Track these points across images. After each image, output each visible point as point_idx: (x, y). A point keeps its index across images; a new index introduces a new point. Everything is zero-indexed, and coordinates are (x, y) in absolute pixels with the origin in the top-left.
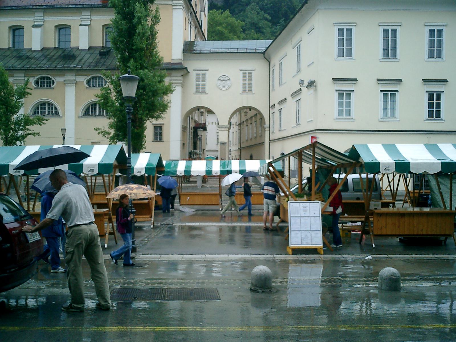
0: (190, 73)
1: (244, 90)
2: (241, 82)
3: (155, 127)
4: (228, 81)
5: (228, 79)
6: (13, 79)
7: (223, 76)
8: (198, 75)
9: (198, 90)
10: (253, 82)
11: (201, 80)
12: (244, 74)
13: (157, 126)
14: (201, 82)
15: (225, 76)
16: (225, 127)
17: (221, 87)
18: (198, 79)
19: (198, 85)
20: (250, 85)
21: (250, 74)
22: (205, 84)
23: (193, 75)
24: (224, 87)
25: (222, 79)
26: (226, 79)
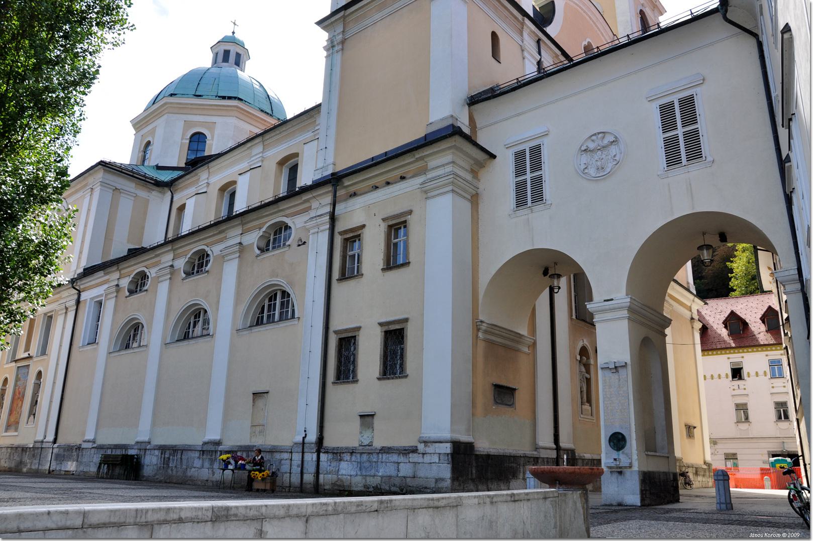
0: (496, 159)
1: (672, 159)
2: (659, 137)
3: (386, 332)
4: (613, 147)
5: (612, 139)
7: (594, 138)
8: (519, 157)
9: (521, 202)
10: (703, 125)
12: (666, 111)
13: (392, 327)
15: (601, 135)
16: (621, 308)
17: (592, 172)
18: (520, 170)
19: (520, 188)
20: (693, 139)
21: (688, 104)
22: (540, 177)
25: (592, 146)
26: (606, 142)
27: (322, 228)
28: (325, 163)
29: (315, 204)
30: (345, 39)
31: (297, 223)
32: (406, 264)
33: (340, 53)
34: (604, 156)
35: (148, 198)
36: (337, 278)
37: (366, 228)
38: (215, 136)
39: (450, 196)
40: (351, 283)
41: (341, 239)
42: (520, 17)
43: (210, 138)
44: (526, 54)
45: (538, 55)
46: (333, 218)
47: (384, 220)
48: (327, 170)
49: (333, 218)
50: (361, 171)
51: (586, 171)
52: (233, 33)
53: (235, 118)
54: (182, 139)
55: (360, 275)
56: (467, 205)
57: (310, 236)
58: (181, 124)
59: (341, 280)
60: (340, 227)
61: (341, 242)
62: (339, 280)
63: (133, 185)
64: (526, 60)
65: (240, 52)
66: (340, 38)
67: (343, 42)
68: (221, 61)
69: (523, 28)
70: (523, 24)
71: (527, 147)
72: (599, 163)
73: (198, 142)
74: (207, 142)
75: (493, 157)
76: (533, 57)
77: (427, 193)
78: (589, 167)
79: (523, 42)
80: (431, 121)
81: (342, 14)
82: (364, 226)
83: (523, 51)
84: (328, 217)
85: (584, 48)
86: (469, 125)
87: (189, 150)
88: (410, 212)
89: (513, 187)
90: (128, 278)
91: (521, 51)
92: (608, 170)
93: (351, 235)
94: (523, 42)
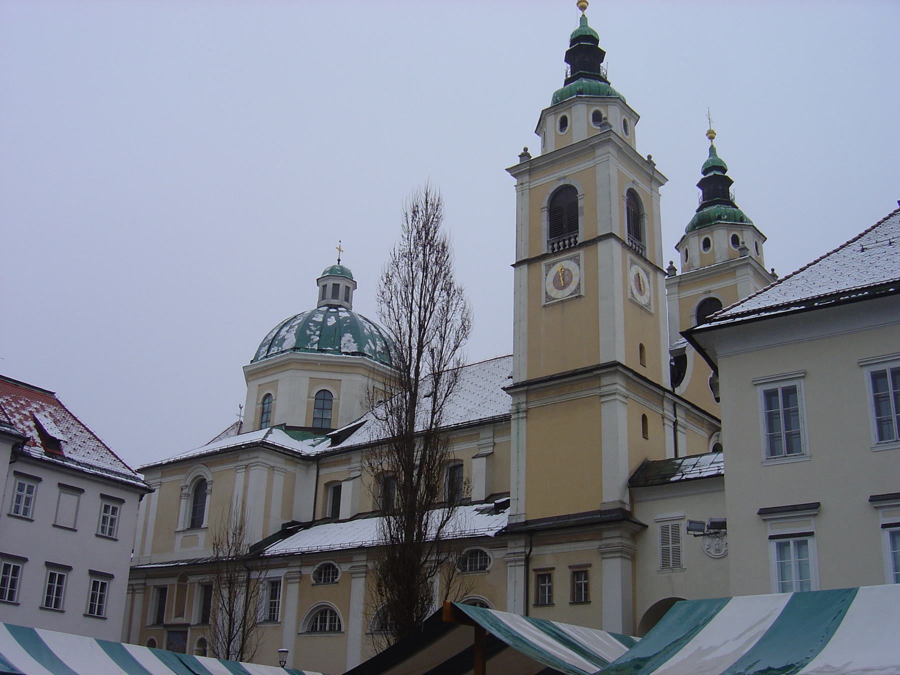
0: (649, 527)
6: (350, 566)
8: (665, 530)
9: (665, 564)
11: (670, 541)
14: (671, 546)
17: (712, 551)
18: (665, 541)
19: (665, 552)
23: (654, 534)
24: (718, 550)
27: (518, 563)
28: (517, 511)
29: (510, 544)
30: (529, 409)
31: (496, 555)
32: (587, 601)
33: (525, 419)
34: (720, 542)
35: (295, 472)
36: (533, 603)
37: (555, 570)
38: (341, 395)
39: (619, 560)
40: (546, 609)
41: (535, 574)
42: (661, 393)
43: (337, 397)
44: (666, 421)
45: (672, 416)
46: (528, 560)
47: (570, 567)
48: (520, 518)
49: (528, 560)
50: (576, 566)
51: (708, 550)
52: (339, 260)
53: (360, 375)
54: (308, 397)
55: (551, 603)
56: (629, 563)
57: (508, 568)
58: (306, 382)
59: (536, 605)
60: (533, 565)
61: (535, 577)
62: (537, 605)
63: (283, 461)
64: (666, 426)
65: (349, 285)
66: (523, 406)
67: (526, 411)
68: (331, 297)
69: (663, 399)
70: (663, 397)
71: (670, 524)
72: (717, 547)
73: (324, 400)
74: (333, 401)
75: (647, 526)
76: (671, 421)
77: (603, 554)
78: (711, 548)
79: (663, 410)
80: (605, 500)
81: (526, 388)
82: (554, 568)
83: (663, 418)
84: (524, 557)
85: (710, 379)
86: (630, 503)
87: (315, 408)
88: (590, 565)
89: (660, 551)
90: (312, 567)
91: (662, 419)
92: (723, 552)
93: (543, 573)
94: (663, 410)
